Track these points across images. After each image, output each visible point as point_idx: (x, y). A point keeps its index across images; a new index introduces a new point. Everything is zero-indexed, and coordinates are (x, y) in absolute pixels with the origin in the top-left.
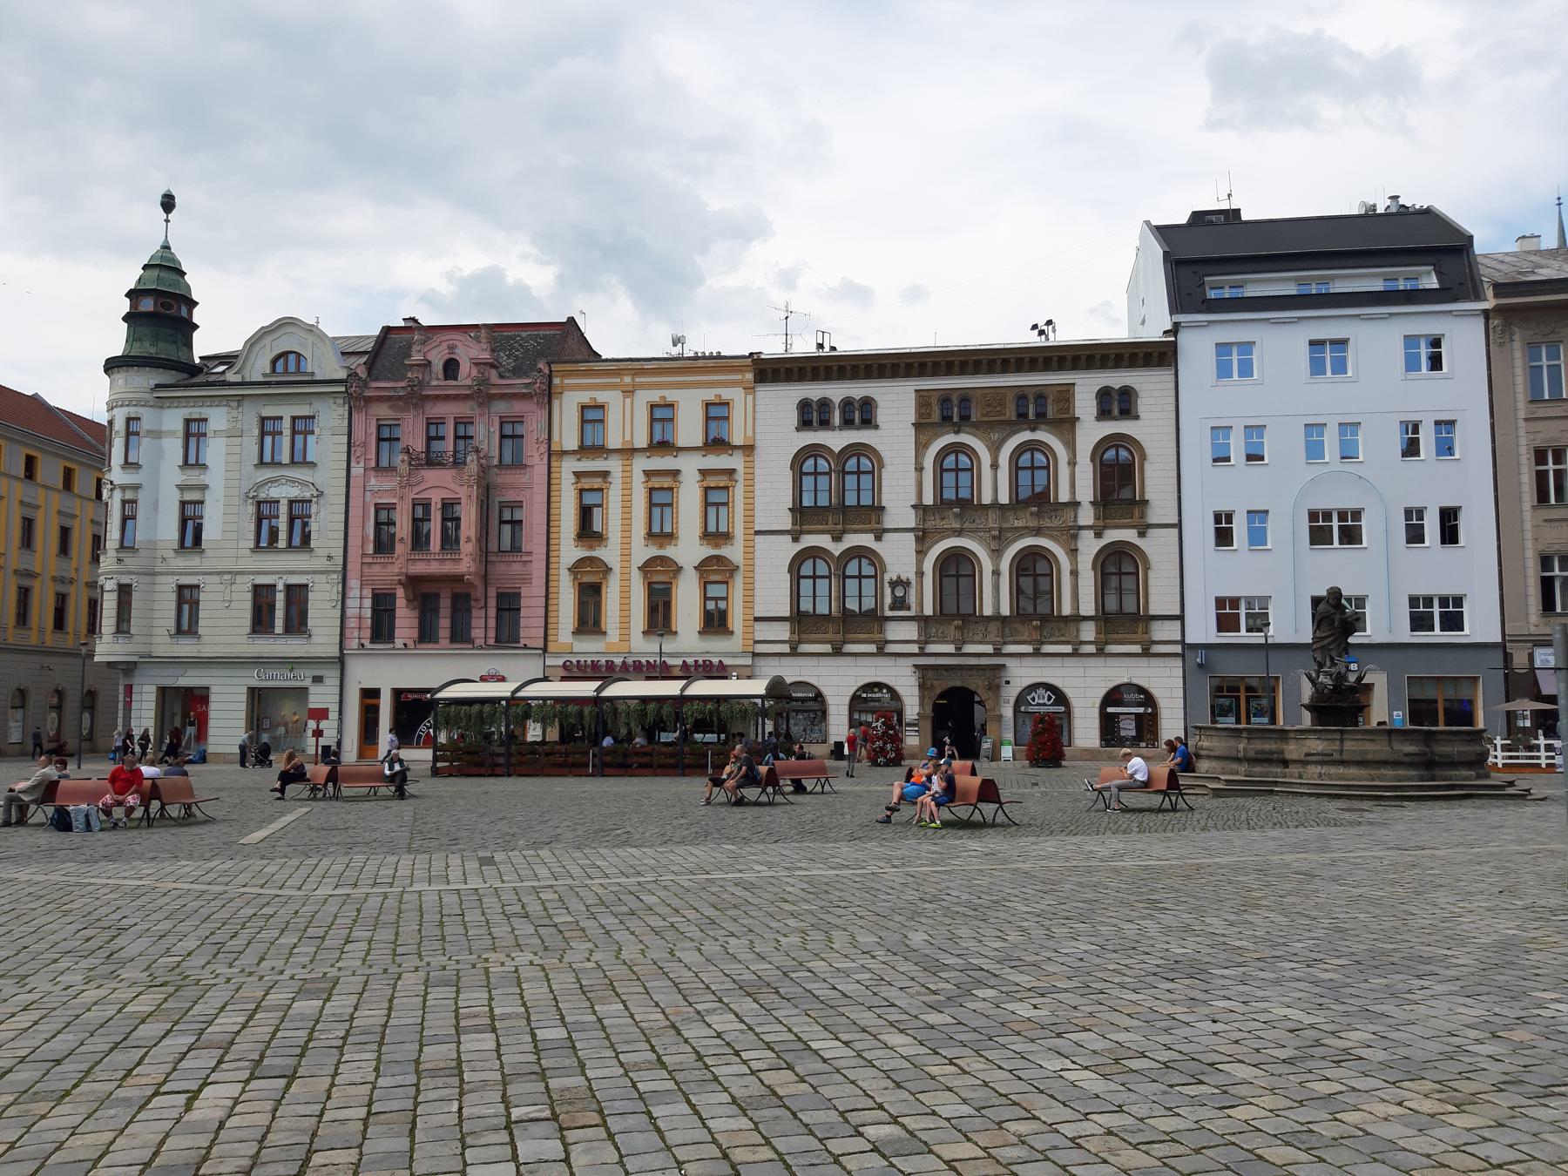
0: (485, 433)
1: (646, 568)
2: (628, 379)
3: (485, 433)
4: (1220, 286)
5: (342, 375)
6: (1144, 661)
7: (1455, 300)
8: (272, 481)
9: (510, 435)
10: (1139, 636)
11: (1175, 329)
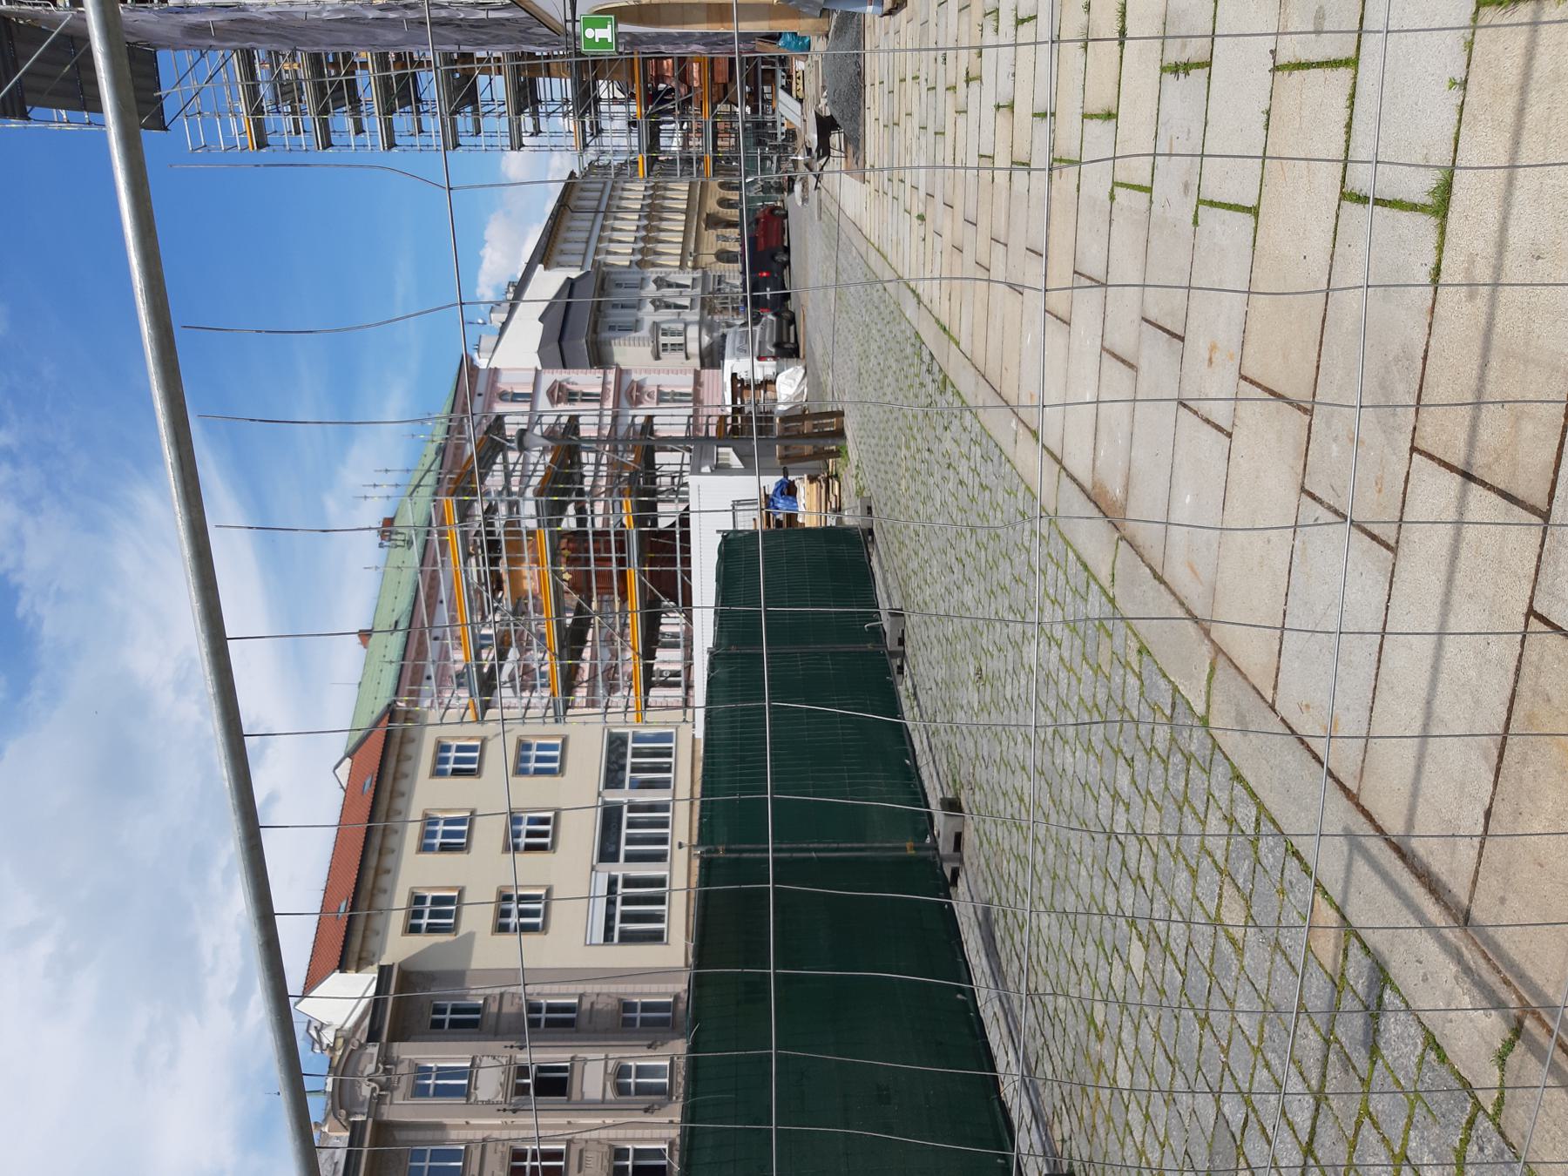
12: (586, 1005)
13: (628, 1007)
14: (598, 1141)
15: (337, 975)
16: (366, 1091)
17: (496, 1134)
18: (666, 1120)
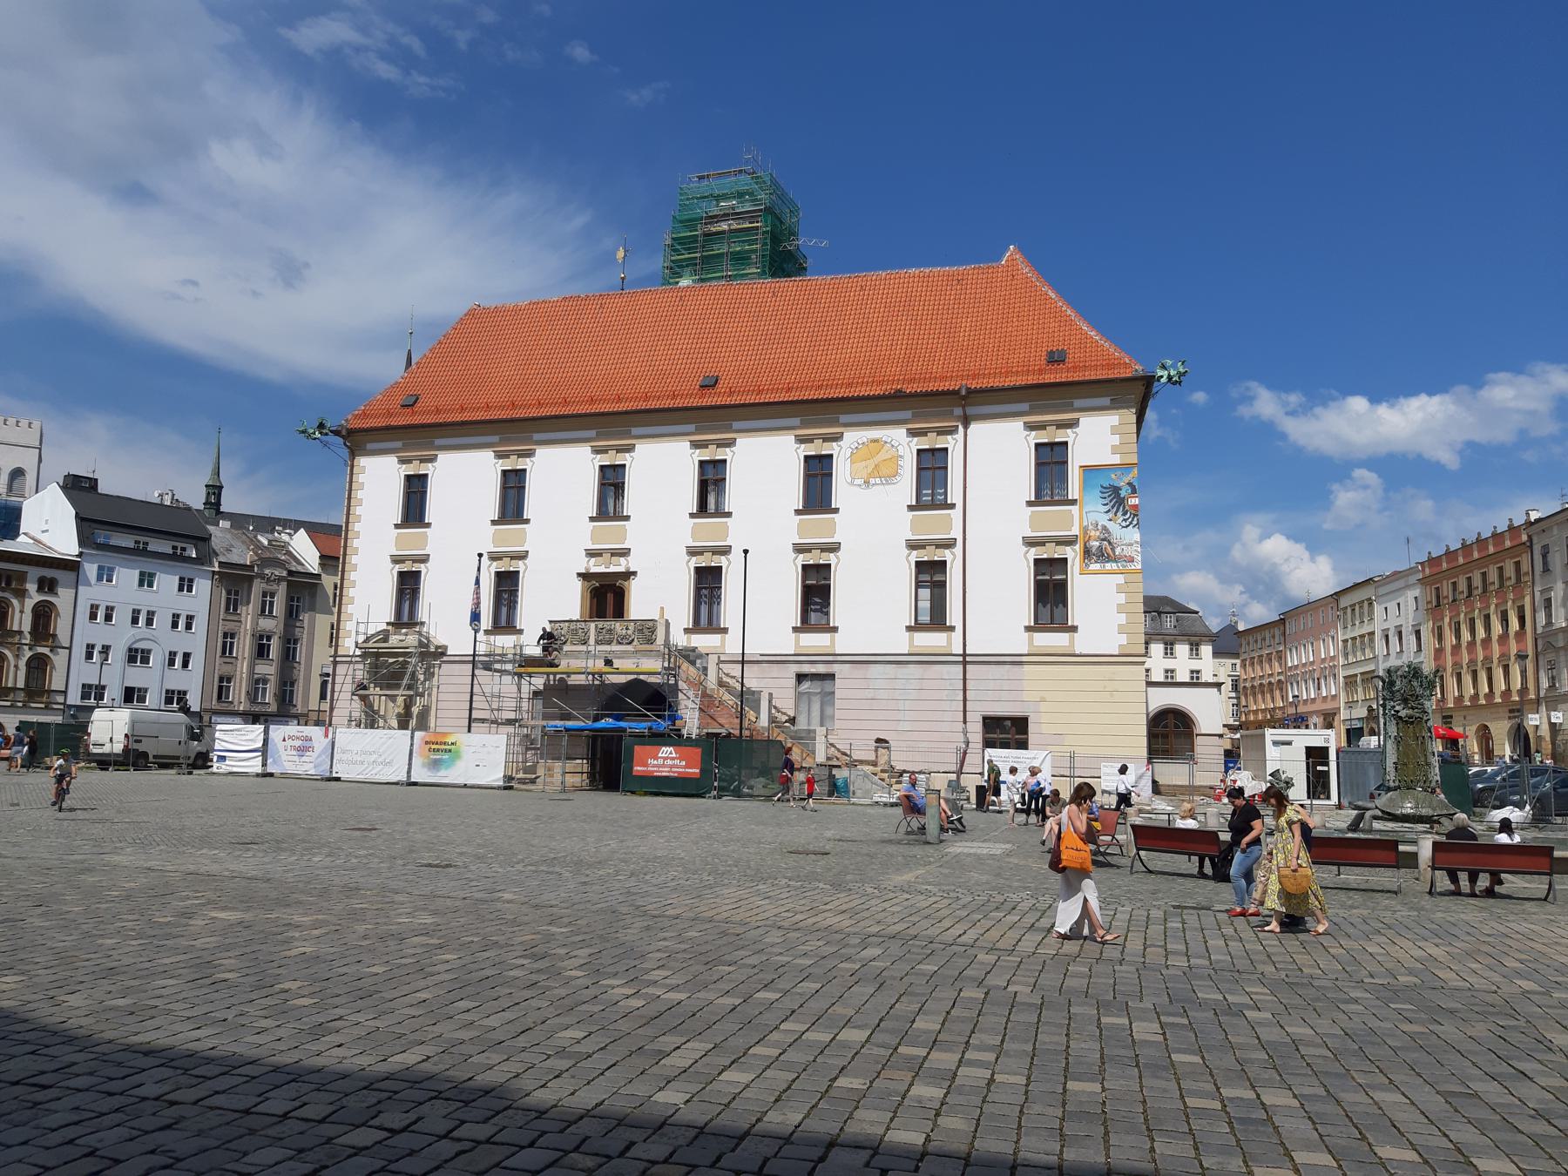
4: (101, 536)
6: (45, 711)
7: (203, 564)
10: (44, 699)
11: (81, 555)
12: (296, 665)
13: (292, 684)
14: (236, 671)
15: (319, 554)
16: (267, 571)
17: (243, 626)
18: (243, 701)
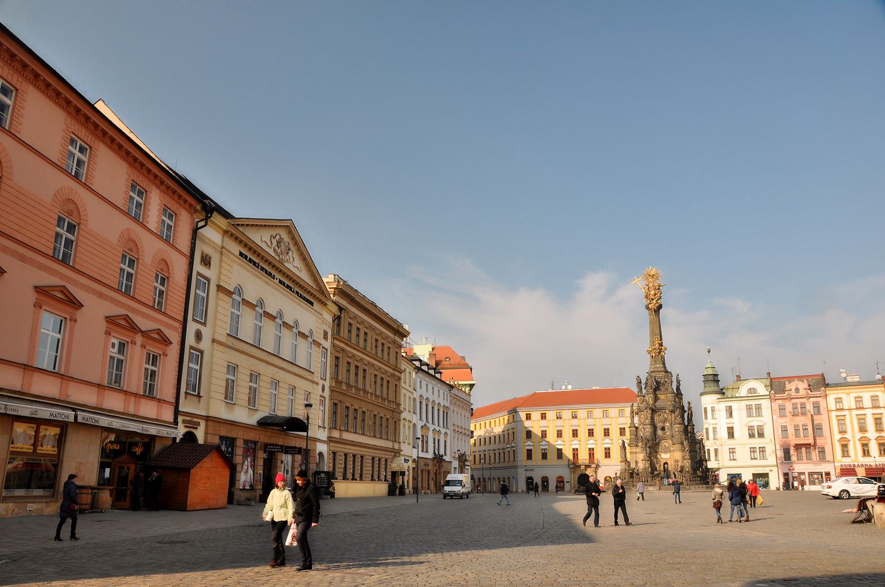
0: (809, 407)
1: (860, 439)
2: (847, 391)
3: (809, 407)
5: (768, 393)
8: (752, 421)
9: (817, 407)
